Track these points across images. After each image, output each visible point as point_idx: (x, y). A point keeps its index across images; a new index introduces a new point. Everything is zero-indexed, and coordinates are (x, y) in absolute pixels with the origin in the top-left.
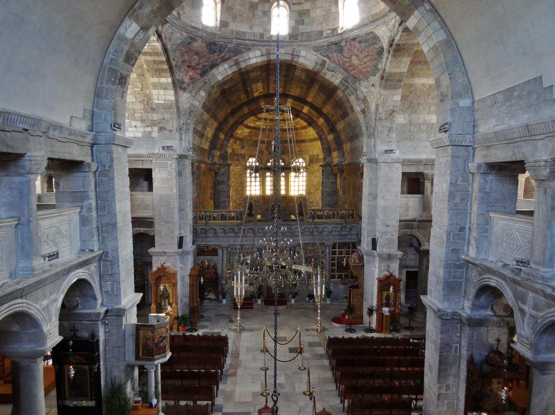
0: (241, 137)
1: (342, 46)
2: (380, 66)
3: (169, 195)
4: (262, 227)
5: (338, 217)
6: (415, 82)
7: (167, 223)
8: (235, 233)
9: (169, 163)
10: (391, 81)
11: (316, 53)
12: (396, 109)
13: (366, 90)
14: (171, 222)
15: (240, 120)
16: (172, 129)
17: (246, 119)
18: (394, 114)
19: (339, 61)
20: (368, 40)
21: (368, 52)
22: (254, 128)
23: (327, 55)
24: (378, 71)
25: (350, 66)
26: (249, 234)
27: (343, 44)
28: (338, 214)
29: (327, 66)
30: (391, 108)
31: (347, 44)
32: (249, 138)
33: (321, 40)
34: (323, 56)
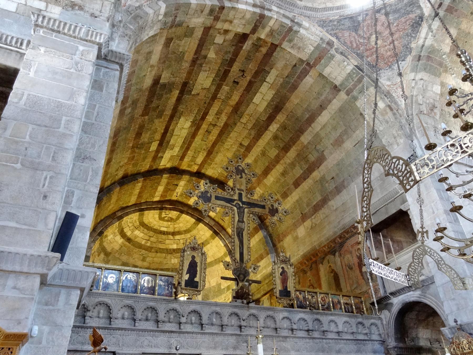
0: (109, 249)
1: (359, 22)
2: (413, 45)
3: (60, 106)
4: (218, 309)
5: (341, 308)
6: (447, 82)
7: (34, 167)
8: (157, 322)
9: (81, 48)
10: (432, 62)
11: (322, 30)
12: (437, 104)
13: (388, 83)
14: (49, 168)
15: (119, 214)
16: (97, 13)
17: (127, 214)
18: (435, 111)
19: (351, 42)
20: (399, 10)
21: (397, 26)
22: (129, 240)
23: (335, 34)
24: (411, 52)
25: (367, 50)
26: (188, 328)
27: (360, 18)
28: (339, 302)
29: (336, 47)
30: (432, 101)
31: (368, 17)
32: (117, 255)
33: (331, 12)
34: (331, 34)
